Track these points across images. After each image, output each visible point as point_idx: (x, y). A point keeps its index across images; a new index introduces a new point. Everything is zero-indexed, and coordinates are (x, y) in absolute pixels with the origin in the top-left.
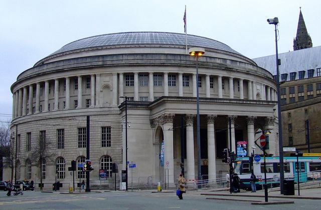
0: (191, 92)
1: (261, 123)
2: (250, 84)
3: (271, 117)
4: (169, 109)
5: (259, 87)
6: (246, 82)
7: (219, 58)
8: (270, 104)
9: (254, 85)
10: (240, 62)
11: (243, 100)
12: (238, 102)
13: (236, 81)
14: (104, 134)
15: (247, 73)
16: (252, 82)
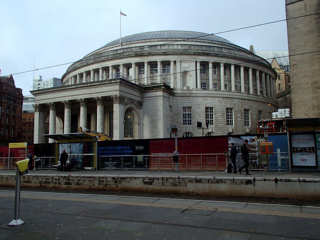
0: (208, 78)
1: (107, 102)
2: (172, 64)
3: (116, 95)
4: (37, 101)
5: (185, 65)
6: (166, 64)
7: (135, 47)
8: (113, 82)
9: (178, 64)
10: (161, 45)
11: (93, 82)
12: (83, 86)
13: (153, 65)
14: (231, 114)
15: (165, 54)
16: (175, 62)
